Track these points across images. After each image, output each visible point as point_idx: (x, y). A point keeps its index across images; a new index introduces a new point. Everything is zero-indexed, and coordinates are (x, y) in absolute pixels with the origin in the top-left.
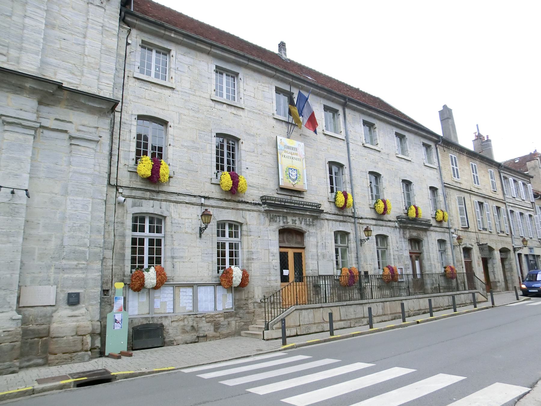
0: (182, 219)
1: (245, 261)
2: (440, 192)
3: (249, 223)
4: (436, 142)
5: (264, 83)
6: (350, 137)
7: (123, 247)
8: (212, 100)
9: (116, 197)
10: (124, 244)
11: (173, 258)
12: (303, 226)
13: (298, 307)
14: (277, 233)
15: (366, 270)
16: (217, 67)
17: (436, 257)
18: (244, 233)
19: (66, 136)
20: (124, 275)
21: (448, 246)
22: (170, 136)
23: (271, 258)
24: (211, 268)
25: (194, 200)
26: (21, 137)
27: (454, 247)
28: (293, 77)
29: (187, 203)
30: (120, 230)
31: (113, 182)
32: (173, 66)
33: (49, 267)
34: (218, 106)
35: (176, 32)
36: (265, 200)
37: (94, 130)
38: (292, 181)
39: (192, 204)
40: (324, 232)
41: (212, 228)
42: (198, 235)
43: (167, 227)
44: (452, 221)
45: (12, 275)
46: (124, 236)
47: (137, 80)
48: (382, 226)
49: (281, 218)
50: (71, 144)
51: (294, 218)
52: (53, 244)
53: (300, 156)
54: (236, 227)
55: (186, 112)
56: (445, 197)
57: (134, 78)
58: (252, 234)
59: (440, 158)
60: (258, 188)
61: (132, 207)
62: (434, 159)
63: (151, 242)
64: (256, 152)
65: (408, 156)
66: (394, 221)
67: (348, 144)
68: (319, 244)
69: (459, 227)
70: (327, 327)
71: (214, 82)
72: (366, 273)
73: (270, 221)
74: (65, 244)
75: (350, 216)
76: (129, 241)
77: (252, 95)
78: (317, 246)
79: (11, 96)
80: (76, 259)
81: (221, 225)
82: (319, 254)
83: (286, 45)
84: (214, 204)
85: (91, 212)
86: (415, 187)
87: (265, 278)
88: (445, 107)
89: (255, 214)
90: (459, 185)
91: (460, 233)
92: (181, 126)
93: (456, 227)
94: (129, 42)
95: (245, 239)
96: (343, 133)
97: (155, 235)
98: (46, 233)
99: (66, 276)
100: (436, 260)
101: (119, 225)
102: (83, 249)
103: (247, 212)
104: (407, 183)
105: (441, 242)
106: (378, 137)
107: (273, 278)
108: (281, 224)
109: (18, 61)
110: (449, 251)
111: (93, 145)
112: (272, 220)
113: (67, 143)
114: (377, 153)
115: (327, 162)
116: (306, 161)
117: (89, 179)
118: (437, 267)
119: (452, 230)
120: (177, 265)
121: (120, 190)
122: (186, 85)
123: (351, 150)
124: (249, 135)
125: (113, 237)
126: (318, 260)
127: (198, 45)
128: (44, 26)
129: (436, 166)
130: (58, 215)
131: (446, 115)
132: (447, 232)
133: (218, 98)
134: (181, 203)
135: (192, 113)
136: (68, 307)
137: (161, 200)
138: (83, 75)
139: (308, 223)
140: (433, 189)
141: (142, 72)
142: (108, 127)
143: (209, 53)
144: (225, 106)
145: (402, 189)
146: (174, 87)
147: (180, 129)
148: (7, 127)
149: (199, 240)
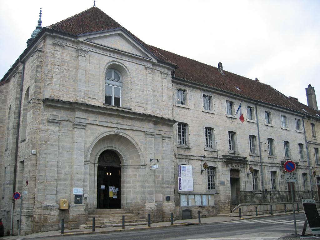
1: (218, 184)
2: (304, 146)
3: (219, 167)
4: (303, 118)
6: (259, 121)
12: (239, 168)
13: (242, 204)
14: (229, 171)
16: (203, 95)
17: (301, 183)
19: (160, 136)
21: (308, 176)
22: (189, 131)
23: (227, 183)
25: (199, 158)
26: (151, 139)
27: (311, 177)
28: (234, 95)
29: (197, 160)
32: (188, 98)
34: (205, 114)
35: (189, 82)
37: (169, 133)
39: (198, 160)
42: (201, 173)
44: (311, 163)
47: (177, 107)
48: (274, 166)
49: (231, 164)
50: (163, 140)
51: (236, 164)
55: (194, 119)
56: (307, 149)
59: (305, 126)
60: (221, 151)
62: (302, 127)
65: (287, 127)
66: (280, 164)
67: (258, 125)
69: (314, 166)
70: (255, 213)
72: (266, 190)
73: (227, 166)
79: (147, 123)
80: (168, 184)
82: (246, 181)
83: (223, 65)
84: (206, 160)
86: (291, 145)
88: (310, 86)
89: (220, 163)
90: (316, 141)
91: (315, 169)
93: (313, 165)
96: (256, 120)
99: (165, 190)
100: (301, 184)
103: (218, 163)
104: (286, 143)
105: (305, 174)
106: (272, 119)
107: (228, 192)
108: (231, 167)
109: (147, 109)
110: (309, 179)
111: (169, 139)
112: (227, 166)
113: (161, 139)
114: (272, 128)
115: (249, 136)
118: (302, 188)
119: (311, 168)
122: (193, 106)
127: (197, 86)
129: (302, 131)
131: (310, 91)
132: (308, 169)
136: (166, 202)
137: (188, 159)
138: (163, 110)
139: (241, 166)
140: (301, 145)
143: (200, 89)
145: (284, 146)
146: (189, 108)
148: (147, 136)
149: (201, 175)
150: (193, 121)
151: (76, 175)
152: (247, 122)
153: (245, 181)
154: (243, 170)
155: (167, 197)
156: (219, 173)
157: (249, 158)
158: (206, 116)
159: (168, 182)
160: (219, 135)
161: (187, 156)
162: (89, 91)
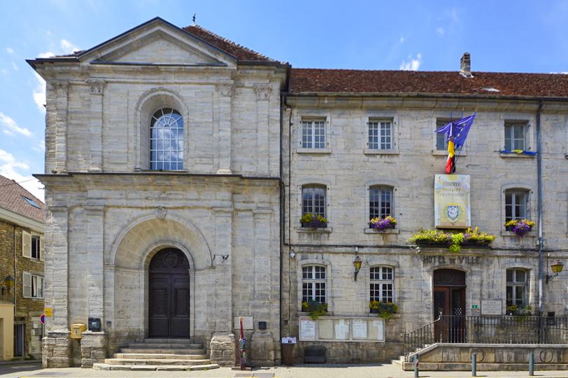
0: (340, 265)
1: (396, 300)
5: (421, 119)
7: (296, 291)
8: (366, 155)
9: (290, 254)
10: (296, 287)
11: (333, 297)
12: (464, 266)
15: (551, 310)
18: (397, 275)
19: (250, 213)
20: (298, 311)
23: (424, 297)
24: (364, 306)
25: (349, 249)
30: (294, 277)
31: (287, 242)
32: (329, 132)
33: (248, 305)
34: (371, 159)
38: (451, 220)
40: (492, 271)
41: (365, 273)
42: (353, 279)
43: (328, 273)
45: (227, 309)
46: (296, 282)
52: (250, 289)
53: (464, 190)
54: (390, 270)
55: (341, 172)
57: (299, 153)
58: (404, 275)
61: (302, 259)
63: (317, 285)
64: (411, 194)
68: (485, 283)
71: (367, 135)
72: (551, 314)
73: (424, 262)
74: (256, 290)
75: (532, 250)
76: (300, 286)
77: (409, 136)
78: (481, 285)
81: (374, 270)
84: (367, 252)
85: (271, 267)
87: (416, 315)
92: (337, 187)
94: (292, 122)
95: (397, 280)
97: (320, 281)
98: (246, 282)
101: (293, 274)
102: (266, 292)
112: (426, 260)
116: (471, 196)
117: (268, 243)
120: (336, 303)
121: (292, 248)
123: (543, 168)
124: (404, 180)
125: (288, 283)
126: (481, 299)
128: (230, 133)
130: (251, 271)
133: (372, 151)
134: (338, 253)
135: (347, 172)
141: (304, 146)
142: (278, 201)
144: (378, 156)
146: (330, 152)
147: (336, 189)
150: (339, 177)
151: (91, 288)
152: (501, 159)
153: (481, 295)
154: (475, 268)
155: (260, 323)
156: (403, 277)
157: (498, 242)
158: (374, 162)
159: (264, 297)
160: (408, 199)
161: (320, 246)
162: (109, 152)
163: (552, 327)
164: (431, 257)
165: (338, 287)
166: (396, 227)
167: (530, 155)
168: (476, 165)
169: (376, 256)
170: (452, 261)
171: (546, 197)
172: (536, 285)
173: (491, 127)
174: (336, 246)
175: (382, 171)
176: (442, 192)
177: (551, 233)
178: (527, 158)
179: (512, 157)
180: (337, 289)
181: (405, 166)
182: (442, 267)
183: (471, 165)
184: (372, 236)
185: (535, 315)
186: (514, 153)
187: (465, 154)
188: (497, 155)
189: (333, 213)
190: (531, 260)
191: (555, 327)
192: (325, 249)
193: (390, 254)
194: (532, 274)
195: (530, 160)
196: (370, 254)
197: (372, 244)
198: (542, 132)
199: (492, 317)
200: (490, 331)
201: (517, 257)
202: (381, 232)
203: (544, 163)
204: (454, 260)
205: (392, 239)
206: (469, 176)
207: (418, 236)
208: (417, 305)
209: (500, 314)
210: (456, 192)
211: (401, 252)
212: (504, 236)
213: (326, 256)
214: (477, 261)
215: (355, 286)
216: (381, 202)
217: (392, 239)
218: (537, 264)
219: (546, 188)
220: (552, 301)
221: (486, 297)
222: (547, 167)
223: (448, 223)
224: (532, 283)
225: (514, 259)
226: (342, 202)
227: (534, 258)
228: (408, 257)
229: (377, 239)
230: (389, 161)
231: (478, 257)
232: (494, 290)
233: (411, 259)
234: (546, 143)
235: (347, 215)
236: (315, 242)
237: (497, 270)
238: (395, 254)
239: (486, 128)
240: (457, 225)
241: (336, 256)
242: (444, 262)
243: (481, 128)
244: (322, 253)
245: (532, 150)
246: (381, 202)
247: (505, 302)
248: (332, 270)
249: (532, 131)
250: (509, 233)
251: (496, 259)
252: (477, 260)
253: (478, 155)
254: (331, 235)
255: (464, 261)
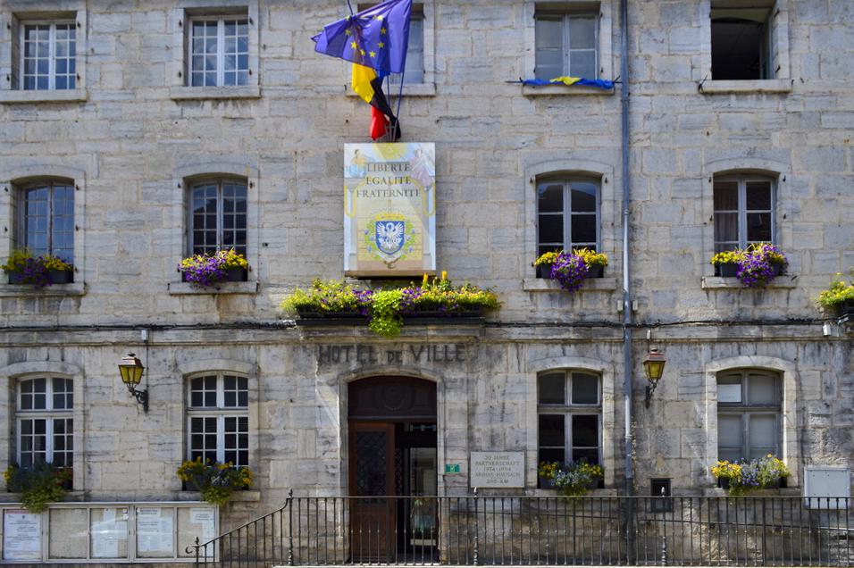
12: (426, 368)
15: (661, 474)
25: (128, 335)
36: (309, 315)
68: (481, 409)
73: (321, 362)
77: (287, 52)
112: (327, 357)
124: (273, 160)
152: (527, 101)
153: (471, 438)
154: (454, 374)
156: (268, 400)
157: (515, 305)
161: (57, 329)
163: (660, 516)
164: (338, 349)
165: (101, 429)
166: (249, 275)
167: (603, 89)
168: (461, 119)
169: (199, 350)
170: (394, 356)
171: (645, 192)
172: (616, 412)
173: (498, 24)
174: (98, 328)
175: (217, 141)
176: (363, 186)
177: (658, 280)
178: (595, 95)
179: (554, 96)
180: (98, 434)
181: (277, 126)
182: (367, 373)
183: (447, 118)
184: (189, 300)
185: (615, 486)
186: (556, 84)
187: (432, 92)
188: (516, 90)
189: (91, 249)
190: (604, 349)
191: (668, 516)
192: (67, 337)
193: (236, 344)
194: (607, 383)
195: (601, 99)
196: (185, 345)
197: (189, 319)
198: (636, 32)
199: (501, 494)
200: (495, 529)
201: (566, 342)
202: (211, 290)
203: (641, 105)
204: (399, 353)
205: (242, 307)
206: (432, 146)
207: (306, 296)
208: (305, 467)
209: (521, 485)
210: (398, 187)
211: (259, 338)
212: (532, 292)
213: (70, 353)
214: (457, 356)
215: (145, 423)
216: (216, 214)
217: (242, 307)
218: (620, 358)
219: (645, 171)
220: (663, 451)
221: (484, 444)
222: (648, 117)
223: (377, 262)
224: (607, 406)
225: (558, 348)
226: (113, 219)
227: (611, 343)
228: (282, 351)
229: (204, 308)
230: (235, 114)
231: (460, 346)
232: (507, 426)
233: (291, 356)
234: (647, 58)
235: (128, 251)
236: (44, 321)
237: (514, 375)
238: (247, 344)
239: (487, 25)
240: (401, 268)
241: (97, 352)
242: (373, 361)
243: (474, 25)
244: (62, 346)
245: (607, 76)
246: (216, 214)
247: (533, 455)
248: (85, 387)
249: (607, 29)
250: (542, 284)
251: (511, 350)
252: (458, 352)
253: (465, 92)
254: (83, 300)
255: (424, 355)
